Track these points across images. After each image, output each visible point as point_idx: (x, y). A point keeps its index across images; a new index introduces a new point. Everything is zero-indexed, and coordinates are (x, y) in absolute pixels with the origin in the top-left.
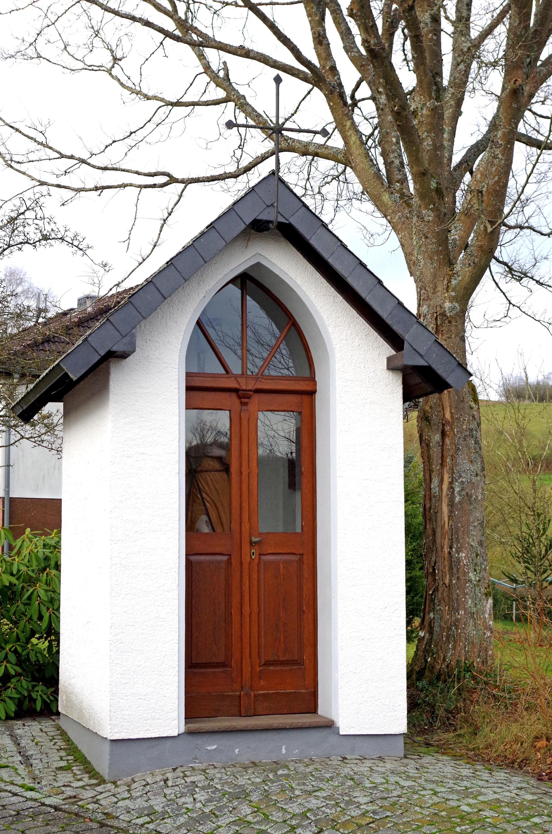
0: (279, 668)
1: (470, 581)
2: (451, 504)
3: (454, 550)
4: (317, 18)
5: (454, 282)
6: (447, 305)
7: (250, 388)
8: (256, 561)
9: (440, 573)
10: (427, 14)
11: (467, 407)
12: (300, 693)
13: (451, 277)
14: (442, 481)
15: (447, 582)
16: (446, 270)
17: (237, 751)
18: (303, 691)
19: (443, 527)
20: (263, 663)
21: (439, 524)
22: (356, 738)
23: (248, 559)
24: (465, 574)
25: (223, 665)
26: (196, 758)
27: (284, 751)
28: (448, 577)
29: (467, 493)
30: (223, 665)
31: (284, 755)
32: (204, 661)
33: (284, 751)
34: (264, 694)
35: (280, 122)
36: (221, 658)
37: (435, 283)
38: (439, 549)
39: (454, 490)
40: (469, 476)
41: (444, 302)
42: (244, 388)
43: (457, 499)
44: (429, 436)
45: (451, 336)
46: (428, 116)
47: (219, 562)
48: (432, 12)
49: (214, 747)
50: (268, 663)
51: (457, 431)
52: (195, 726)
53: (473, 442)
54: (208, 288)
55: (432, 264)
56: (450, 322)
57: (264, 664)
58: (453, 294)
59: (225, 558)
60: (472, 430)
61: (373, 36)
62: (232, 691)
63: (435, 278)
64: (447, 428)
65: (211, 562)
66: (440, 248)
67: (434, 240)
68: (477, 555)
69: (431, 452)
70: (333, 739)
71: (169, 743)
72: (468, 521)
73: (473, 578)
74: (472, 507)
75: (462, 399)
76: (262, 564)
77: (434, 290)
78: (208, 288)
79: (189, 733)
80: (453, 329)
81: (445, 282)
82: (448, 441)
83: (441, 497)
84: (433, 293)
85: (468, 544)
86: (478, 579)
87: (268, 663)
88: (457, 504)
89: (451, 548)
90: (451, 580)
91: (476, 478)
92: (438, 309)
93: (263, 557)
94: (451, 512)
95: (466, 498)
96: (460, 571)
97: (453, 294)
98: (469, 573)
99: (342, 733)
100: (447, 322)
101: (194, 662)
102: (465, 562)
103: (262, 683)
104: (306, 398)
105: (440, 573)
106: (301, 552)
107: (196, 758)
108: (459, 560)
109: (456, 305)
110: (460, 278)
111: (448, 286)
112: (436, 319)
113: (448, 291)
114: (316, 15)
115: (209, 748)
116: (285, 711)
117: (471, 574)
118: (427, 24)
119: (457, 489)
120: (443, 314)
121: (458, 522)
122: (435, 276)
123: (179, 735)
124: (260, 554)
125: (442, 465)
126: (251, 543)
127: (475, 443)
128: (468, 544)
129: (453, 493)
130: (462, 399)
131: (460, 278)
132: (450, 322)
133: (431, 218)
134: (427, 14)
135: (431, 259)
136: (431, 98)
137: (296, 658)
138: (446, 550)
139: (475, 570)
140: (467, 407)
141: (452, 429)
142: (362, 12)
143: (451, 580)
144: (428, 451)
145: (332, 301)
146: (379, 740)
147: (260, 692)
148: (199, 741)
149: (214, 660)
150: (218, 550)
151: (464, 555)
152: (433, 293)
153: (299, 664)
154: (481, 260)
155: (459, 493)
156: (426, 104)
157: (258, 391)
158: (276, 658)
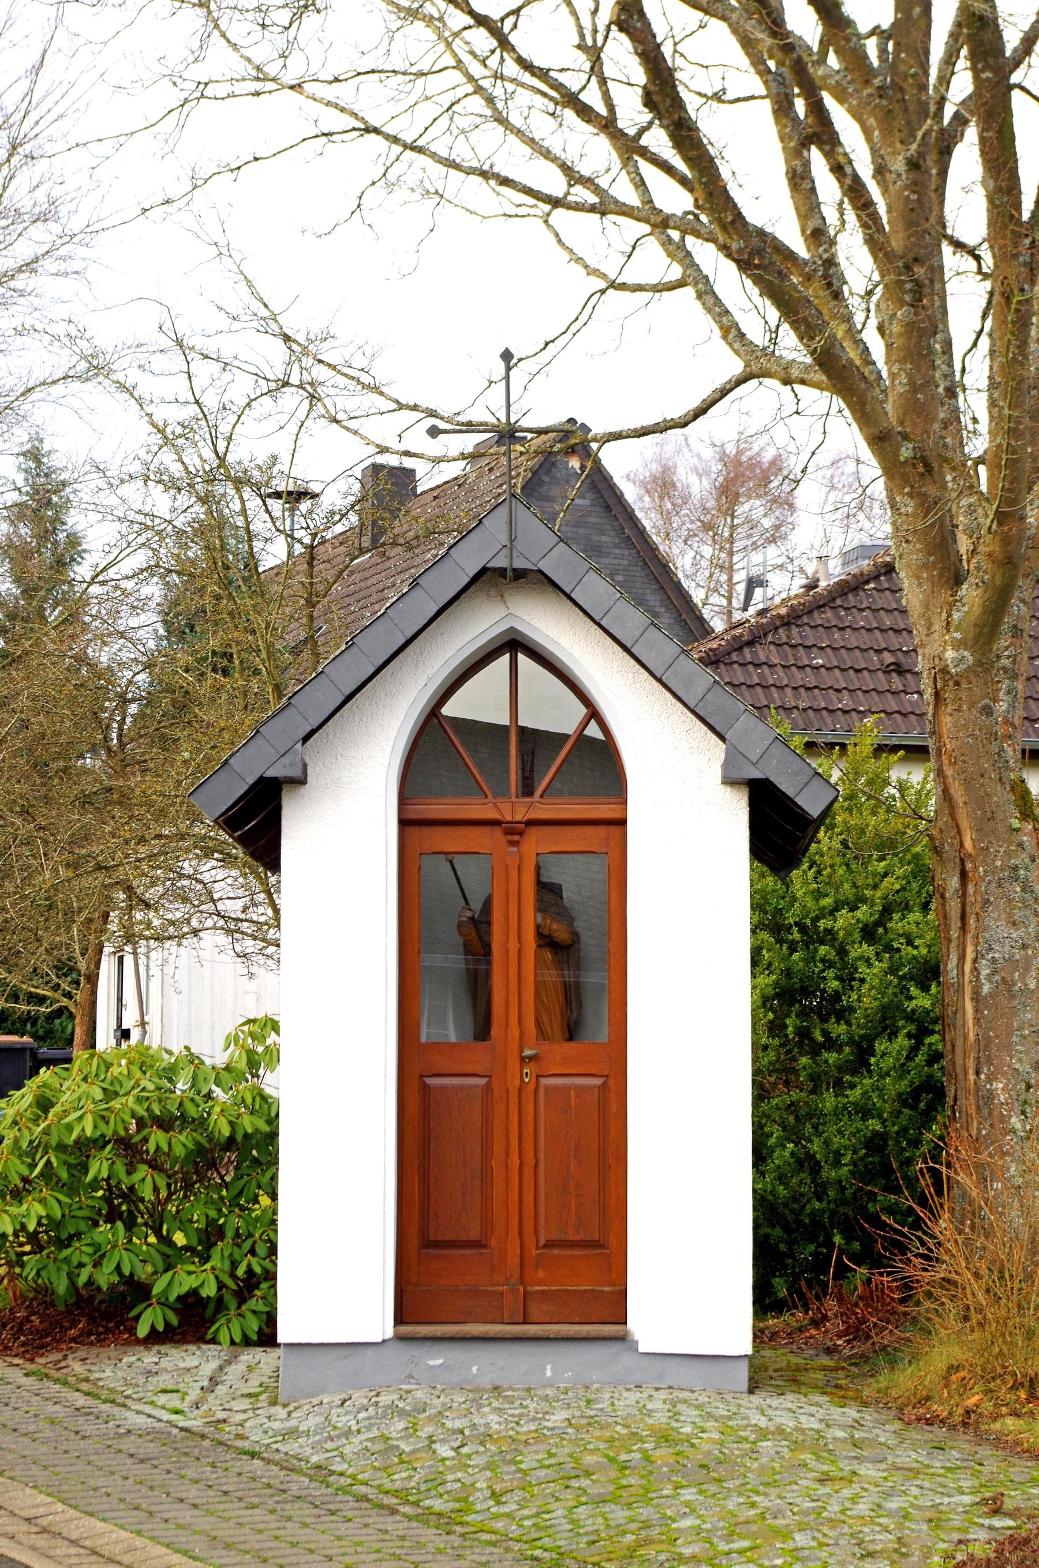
0: (569, 1252)
1: (1013, 1131)
2: (977, 998)
3: (983, 1076)
4: (792, 144)
5: (956, 616)
6: (950, 654)
7: (518, 818)
8: (532, 1087)
9: (964, 1117)
10: (900, 158)
11: (1002, 830)
12: (602, 1291)
13: (952, 605)
14: (962, 958)
15: (974, 1132)
16: (945, 595)
17: (474, 1369)
18: (607, 1289)
19: (966, 1037)
20: (542, 1242)
21: (959, 1032)
22: (668, 1360)
23: (517, 1083)
24: (1003, 1119)
25: (478, 1244)
26: (411, 1376)
27: (549, 1373)
28: (975, 1125)
29: (1003, 979)
30: (478, 1244)
31: (549, 1379)
32: (447, 1238)
33: (549, 1373)
34: (543, 1292)
35: (512, 421)
36: (474, 1235)
37: (929, 619)
38: (961, 1076)
39: (979, 973)
40: (1007, 948)
41: (945, 650)
42: (509, 818)
43: (986, 989)
44: (944, 880)
45: (960, 706)
46: (901, 334)
47: (472, 1087)
48: (909, 154)
49: (440, 1361)
50: (550, 1244)
51: (985, 871)
52: (405, 1329)
53: (1018, 889)
54: (430, 672)
55: (920, 585)
56: (957, 683)
57: (545, 1246)
58: (958, 635)
59: (482, 1081)
60: (1016, 868)
61: (735, 237)
62: (493, 1285)
63: (928, 609)
64: (969, 866)
65: (461, 1087)
66: (932, 558)
67: (918, 546)
68: (1029, 1087)
69: (948, 908)
70: (626, 1359)
71: (370, 1352)
72: (1008, 1026)
73: (1018, 1126)
74: (1015, 1003)
75: (989, 815)
76: (542, 1091)
77: (928, 629)
78: (430, 672)
79: (399, 1338)
80: (963, 695)
81: (944, 615)
82: (971, 889)
83: (960, 986)
84: (927, 635)
85: (1009, 1066)
86: (1028, 1127)
87: (550, 1244)
88: (985, 997)
89: (978, 1073)
90: (979, 1130)
91: (1022, 952)
92: (937, 661)
93: (543, 1081)
94: (976, 1011)
95: (1002, 987)
96: (995, 1113)
97: (958, 635)
98: (1010, 1117)
99: (641, 1349)
100: (951, 683)
101: (432, 1238)
102: (1002, 1098)
103: (541, 1274)
104: (613, 829)
105: (964, 1117)
106: (606, 1073)
107: (411, 1376)
108: (991, 1095)
109: (966, 653)
110: (966, 609)
111: (948, 623)
112: (935, 678)
113: (948, 631)
114: (791, 138)
115: (432, 1363)
116: (577, 1320)
117: (1014, 1120)
118: (899, 175)
119: (985, 972)
120: (945, 671)
121: (990, 1029)
122: (927, 606)
123: (384, 1341)
124: (538, 1076)
125: (964, 928)
126: (522, 1059)
127: (1023, 890)
128: (1009, 1066)
129: (978, 978)
130: (989, 815)
131: (966, 609)
132: (957, 683)
133: (910, 510)
134: (900, 158)
135: (918, 578)
136: (902, 303)
137: (596, 1238)
138: (972, 1077)
139: (1023, 1113)
140: (1002, 830)
141: (976, 868)
142: (712, 203)
143: (979, 1130)
144: (944, 905)
145: (631, 680)
146: (707, 1364)
147: (537, 1288)
148: (416, 1351)
149: (463, 1237)
150: (470, 1069)
151: (1001, 1085)
152: (927, 635)
153: (602, 1246)
154: (993, 577)
155: (989, 977)
156: (895, 314)
157: (530, 823)
158: (563, 1237)
